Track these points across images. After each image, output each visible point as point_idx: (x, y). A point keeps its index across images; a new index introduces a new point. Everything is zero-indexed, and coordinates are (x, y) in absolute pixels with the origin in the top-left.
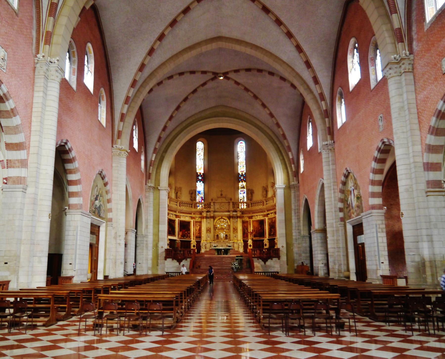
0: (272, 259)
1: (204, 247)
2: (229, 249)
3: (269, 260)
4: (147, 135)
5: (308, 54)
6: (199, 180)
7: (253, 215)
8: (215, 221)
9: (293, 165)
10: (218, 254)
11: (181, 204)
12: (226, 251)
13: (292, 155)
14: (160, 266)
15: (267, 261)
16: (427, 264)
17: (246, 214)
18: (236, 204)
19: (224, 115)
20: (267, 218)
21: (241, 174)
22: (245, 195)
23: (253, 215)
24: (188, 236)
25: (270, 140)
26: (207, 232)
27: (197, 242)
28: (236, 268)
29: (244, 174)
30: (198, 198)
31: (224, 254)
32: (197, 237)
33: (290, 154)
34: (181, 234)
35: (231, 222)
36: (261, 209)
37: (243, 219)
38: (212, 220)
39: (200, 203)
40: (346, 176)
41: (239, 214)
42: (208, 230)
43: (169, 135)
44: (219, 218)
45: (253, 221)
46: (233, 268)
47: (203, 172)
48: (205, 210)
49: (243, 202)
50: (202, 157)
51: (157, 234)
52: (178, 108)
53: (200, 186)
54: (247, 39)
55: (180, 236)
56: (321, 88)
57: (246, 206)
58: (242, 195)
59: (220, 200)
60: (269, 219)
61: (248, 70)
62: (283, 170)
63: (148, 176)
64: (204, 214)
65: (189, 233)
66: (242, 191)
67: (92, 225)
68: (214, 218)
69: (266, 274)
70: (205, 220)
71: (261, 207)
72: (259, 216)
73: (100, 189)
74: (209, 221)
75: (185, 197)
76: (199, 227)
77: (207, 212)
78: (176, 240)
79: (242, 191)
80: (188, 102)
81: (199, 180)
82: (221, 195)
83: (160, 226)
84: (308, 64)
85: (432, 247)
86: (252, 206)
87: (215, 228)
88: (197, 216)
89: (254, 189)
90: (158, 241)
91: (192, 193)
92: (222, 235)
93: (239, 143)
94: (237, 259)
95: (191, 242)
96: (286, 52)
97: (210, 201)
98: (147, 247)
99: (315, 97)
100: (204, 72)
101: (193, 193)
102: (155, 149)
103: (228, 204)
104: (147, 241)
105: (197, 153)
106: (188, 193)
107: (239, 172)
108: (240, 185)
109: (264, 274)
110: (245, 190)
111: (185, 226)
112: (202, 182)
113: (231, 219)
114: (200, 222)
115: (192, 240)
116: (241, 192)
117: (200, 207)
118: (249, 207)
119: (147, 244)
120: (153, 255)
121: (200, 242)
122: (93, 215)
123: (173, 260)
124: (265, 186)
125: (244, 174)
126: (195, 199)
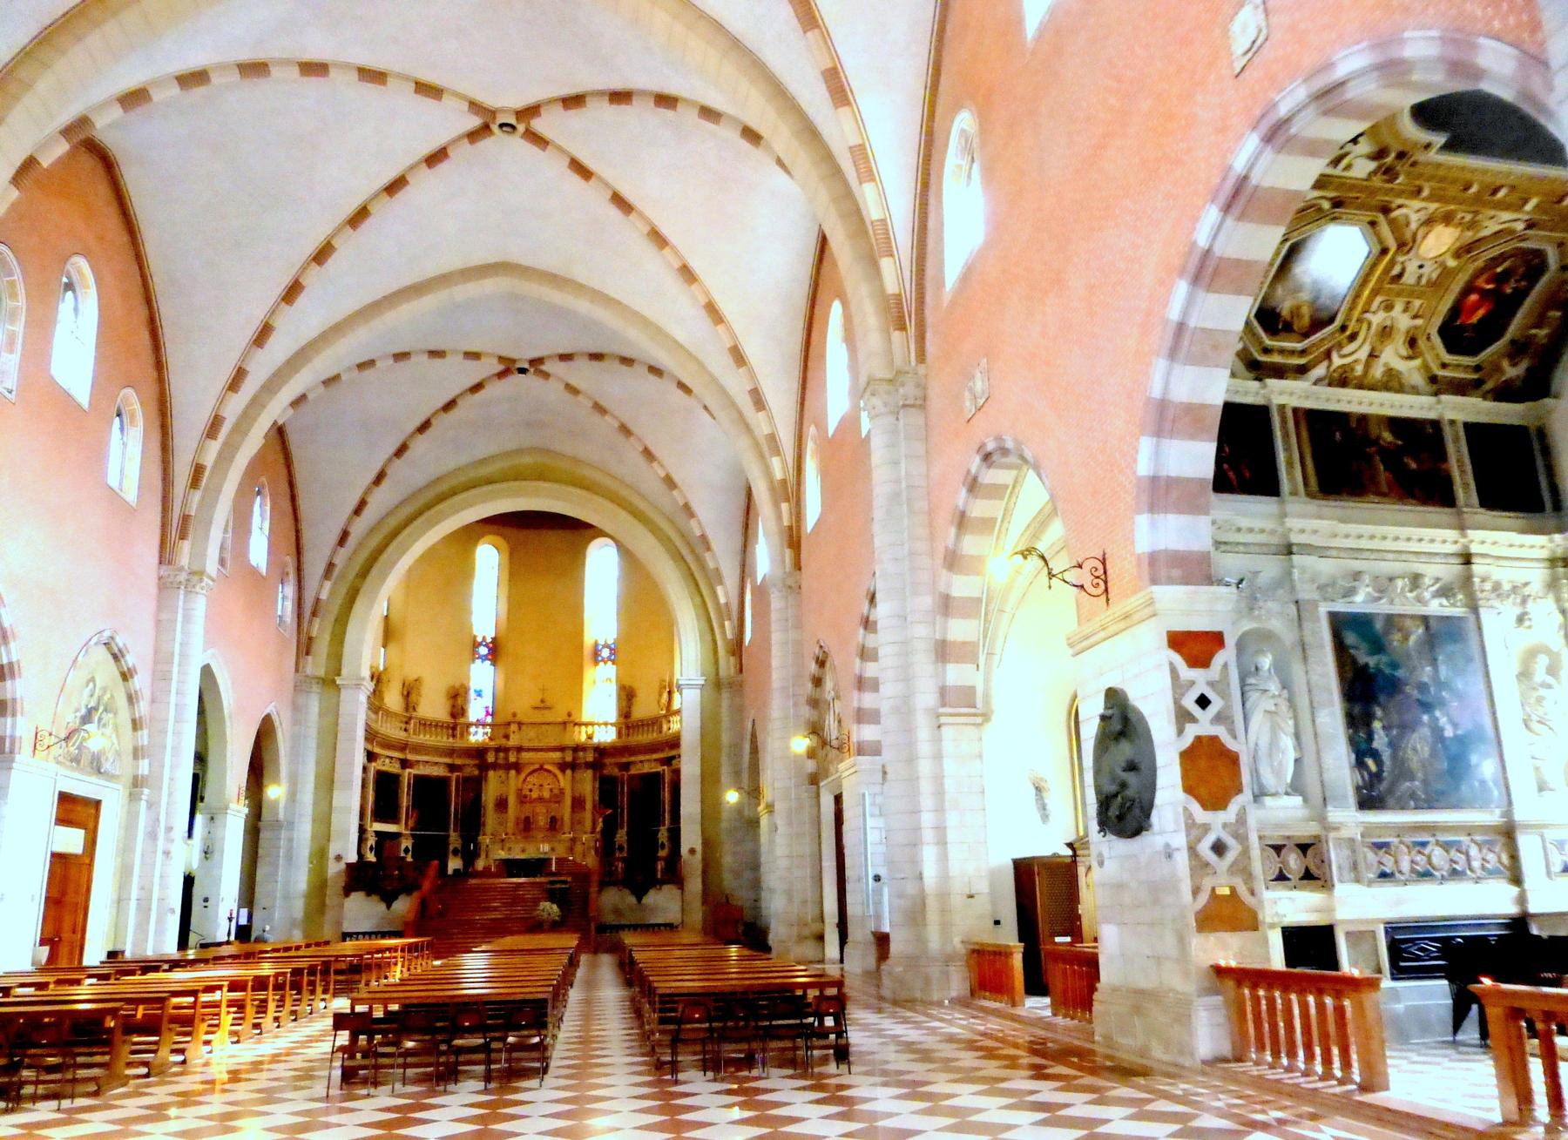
4: (304, 526)
5: (738, 327)
7: (633, 759)
8: (523, 775)
9: (727, 623)
13: (726, 594)
14: (330, 915)
15: (646, 892)
16: (932, 903)
19: (541, 474)
23: (633, 759)
25: (668, 550)
33: (719, 590)
39: (479, 723)
40: (821, 663)
43: (372, 531)
45: (632, 777)
51: (324, 821)
52: (401, 451)
53: (482, 677)
54: (582, 276)
55: (411, 823)
56: (771, 419)
61: (597, 357)
63: (305, 647)
67: (65, 799)
73: (105, 689)
80: (429, 433)
83: (336, 794)
84: (738, 356)
85: (943, 858)
87: (523, 799)
92: (542, 821)
96: (680, 317)
98: (289, 857)
99: (757, 445)
100: (473, 356)
102: (330, 566)
104: (291, 840)
113: (569, 772)
119: (290, 850)
120: (309, 883)
122: (73, 769)
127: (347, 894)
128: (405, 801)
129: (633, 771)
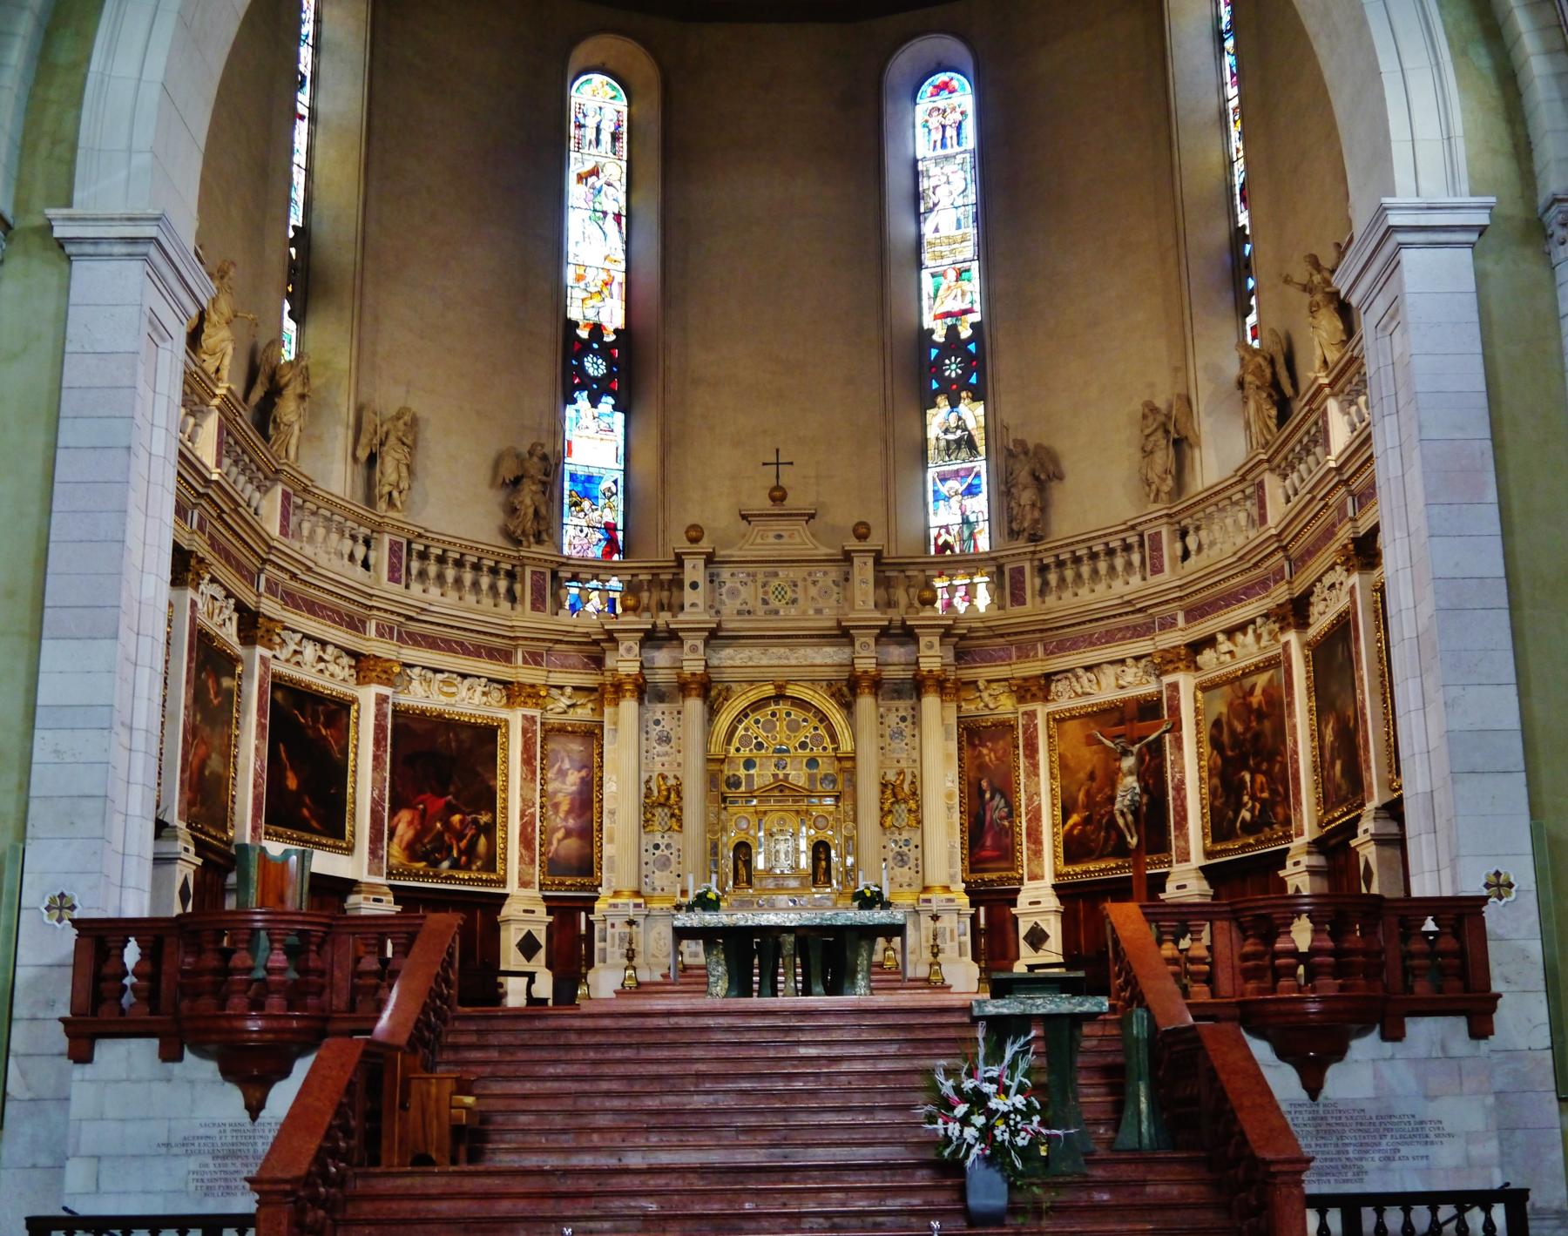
0: (1394, 1034)
1: (616, 954)
2: (869, 933)
3: (1365, 1048)
6: (586, 383)
8: (724, 721)
10: (741, 985)
11: (415, 555)
12: (830, 954)
15: (1339, 1053)
17: (989, 659)
18: (906, 570)
20: (1186, 682)
21: (939, 337)
22: (979, 506)
24: (470, 851)
26: (647, 823)
27: (552, 905)
28: (997, 1155)
29: (965, 333)
30: (579, 535)
31: (807, 991)
32: (553, 867)
34: (405, 826)
35: (866, 732)
36: (1130, 605)
37: (969, 708)
38: (694, 706)
41: (933, 656)
42: (660, 803)
44: (753, 696)
45: (1058, 720)
46: (948, 1167)
47: (618, 321)
48: (631, 620)
49: (971, 563)
50: (615, 200)
53: (594, 438)
55: (395, 852)
57: (997, 586)
58: (956, 507)
59: (762, 541)
60: (1204, 688)
62: (1460, 53)
64: (625, 661)
65: (489, 830)
66: (956, 474)
68: (708, 689)
69: (1368, 1217)
70: (629, 706)
71: (1133, 585)
72: (1109, 675)
74: (667, 724)
75: (453, 501)
76: (574, 778)
77: (650, 639)
78: (350, 886)
79: (956, 474)
81: (586, 383)
82: (778, 495)
86: (1044, 590)
87: (722, 788)
88: (557, 678)
89: (1061, 445)
90: (22, 834)
91: (517, 482)
93: (927, 88)
94: (1002, 1028)
95: (506, 911)
97: (683, 545)
101: (532, 481)
103: (834, 573)
105: (577, 164)
106: (484, 474)
107: (928, 322)
108: (933, 431)
109: (1334, 1219)
110: (981, 465)
111: (444, 768)
112: (607, 402)
113: (865, 703)
114: (592, 734)
115: (512, 887)
116: (944, 489)
117: (592, 605)
118: (1018, 599)
121: (588, 905)
123: (170, 1054)
124: (1161, 403)
125: (965, 333)
126: (545, 527)
127: (81, 1053)
129: (1065, 699)
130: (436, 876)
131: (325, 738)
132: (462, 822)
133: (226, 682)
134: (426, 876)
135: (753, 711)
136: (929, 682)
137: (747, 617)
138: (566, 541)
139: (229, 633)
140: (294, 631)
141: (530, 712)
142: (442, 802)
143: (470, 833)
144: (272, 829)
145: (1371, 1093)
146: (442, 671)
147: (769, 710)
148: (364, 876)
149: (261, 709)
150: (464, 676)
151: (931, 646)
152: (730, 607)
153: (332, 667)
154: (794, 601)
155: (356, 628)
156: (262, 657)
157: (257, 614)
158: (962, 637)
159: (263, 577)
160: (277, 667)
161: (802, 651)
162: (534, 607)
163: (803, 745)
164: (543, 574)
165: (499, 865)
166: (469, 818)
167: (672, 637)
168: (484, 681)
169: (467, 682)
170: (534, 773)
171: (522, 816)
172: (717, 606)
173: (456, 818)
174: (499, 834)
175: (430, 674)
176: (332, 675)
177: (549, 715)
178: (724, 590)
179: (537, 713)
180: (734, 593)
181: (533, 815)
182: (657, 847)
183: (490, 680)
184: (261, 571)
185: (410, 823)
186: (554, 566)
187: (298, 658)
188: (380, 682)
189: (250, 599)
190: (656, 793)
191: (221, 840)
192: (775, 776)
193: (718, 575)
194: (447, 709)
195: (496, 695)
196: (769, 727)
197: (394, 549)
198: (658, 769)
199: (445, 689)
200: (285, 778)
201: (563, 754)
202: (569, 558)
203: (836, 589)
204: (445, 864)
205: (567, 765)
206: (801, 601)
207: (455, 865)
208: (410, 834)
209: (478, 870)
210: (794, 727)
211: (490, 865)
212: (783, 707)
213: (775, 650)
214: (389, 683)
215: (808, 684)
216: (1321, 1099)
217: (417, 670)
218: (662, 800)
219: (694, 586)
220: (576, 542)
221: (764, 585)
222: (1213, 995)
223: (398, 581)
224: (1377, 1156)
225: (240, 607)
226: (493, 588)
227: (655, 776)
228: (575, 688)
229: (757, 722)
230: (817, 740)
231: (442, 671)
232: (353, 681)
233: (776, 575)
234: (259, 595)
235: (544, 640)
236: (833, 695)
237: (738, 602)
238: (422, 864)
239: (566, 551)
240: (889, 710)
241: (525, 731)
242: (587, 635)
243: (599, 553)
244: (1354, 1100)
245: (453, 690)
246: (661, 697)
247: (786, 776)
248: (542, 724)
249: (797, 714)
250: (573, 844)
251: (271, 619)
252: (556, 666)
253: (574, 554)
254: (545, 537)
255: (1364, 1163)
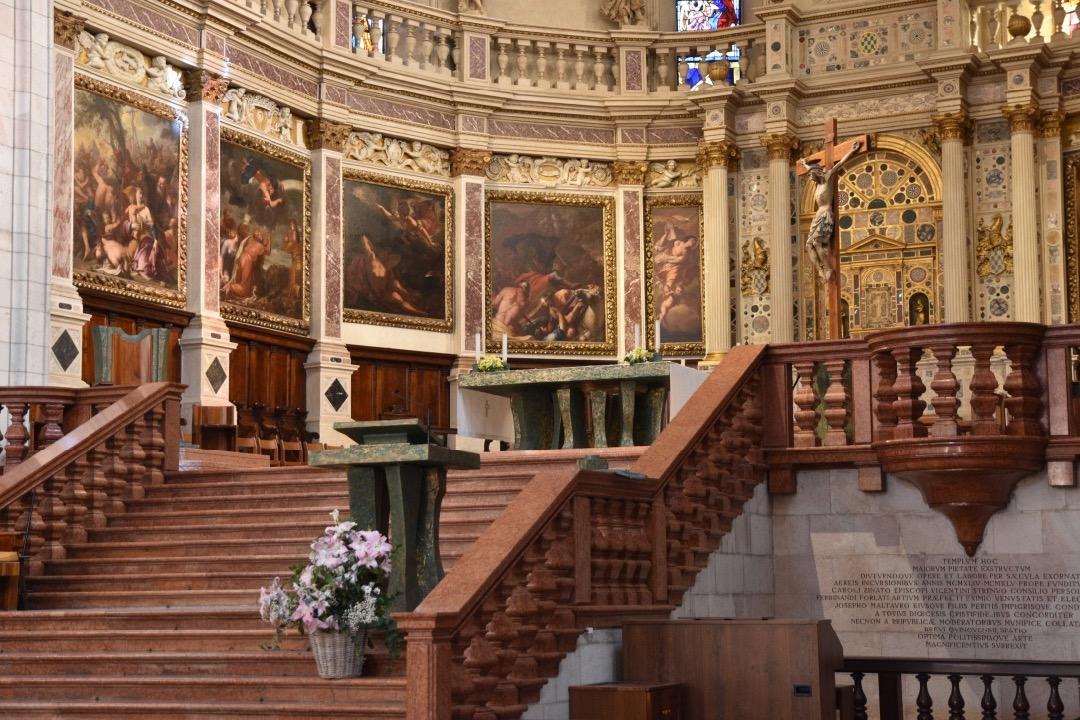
15: (1001, 502)
34: (507, 302)
65: (596, 302)
76: (680, 247)
78: (450, 361)
88: (658, 153)
128: (463, 266)
130: (541, 348)
131: (416, 229)
132: (567, 296)
133: (288, 185)
134: (531, 347)
135: (848, 167)
136: (1018, 118)
137: (837, 72)
138: (680, 16)
139: (292, 142)
140: (372, 133)
141: (631, 188)
142: (546, 278)
143: (576, 305)
144: (356, 312)
145: (1039, 549)
146: (540, 157)
147: (864, 165)
148: (463, 352)
149: (332, 208)
150: (565, 160)
151: (1019, 80)
152: (819, 63)
153: (423, 162)
154: (884, 50)
155: (444, 125)
156: (328, 159)
157: (318, 120)
158: (1066, 66)
159: (324, 86)
160: (345, 165)
161: (892, 101)
162: (629, 87)
163: (899, 198)
164: (637, 53)
165: (608, 334)
166: (575, 292)
167: (757, 103)
168: (584, 162)
169: (568, 165)
170: (637, 246)
171: (627, 288)
172: (808, 64)
173: (561, 293)
174: (608, 305)
175: (528, 161)
176: (423, 170)
177: (654, 189)
178: (812, 48)
179: (639, 189)
180: (823, 50)
181: (638, 285)
182: (755, 309)
183: (591, 161)
184: (320, 81)
185: (514, 300)
186: (648, 44)
187: (382, 156)
188: (470, 171)
189: (309, 106)
190: (753, 258)
191: (300, 327)
192: (872, 232)
193: (808, 33)
194: (548, 192)
195: (600, 174)
196: (865, 182)
197: (476, 46)
198: (755, 232)
199: (545, 173)
200: (372, 267)
201: (669, 226)
202: (685, 32)
203: (926, 30)
204: (551, 336)
205: (673, 236)
206: (891, 49)
207: (562, 336)
208: (514, 310)
209: (586, 340)
210: (889, 180)
211: (599, 333)
212: (878, 161)
213: (864, 102)
214: (480, 172)
215: (901, 134)
216: (979, 554)
217: (514, 158)
218: (758, 265)
219: (776, 47)
220: (691, 16)
221: (853, 38)
222: (850, 441)
223: (482, 76)
224: (1043, 620)
225: (297, 114)
226: (590, 73)
227: (751, 240)
228: (678, 161)
229: (852, 178)
230: (914, 191)
231: (540, 157)
232: (446, 174)
233: (866, 24)
234: (320, 103)
235: (641, 117)
236: (926, 142)
237: (827, 58)
238: (528, 337)
239: (681, 26)
240: (986, 152)
241: (627, 207)
242: (682, 107)
243: (715, 24)
244: (1018, 556)
245: (555, 173)
246: (755, 162)
247: (883, 231)
248: (645, 199)
249: (893, 167)
250: (680, 308)
251: (335, 123)
252: (657, 141)
253: (689, 28)
254: (639, 14)
255: (1027, 627)
